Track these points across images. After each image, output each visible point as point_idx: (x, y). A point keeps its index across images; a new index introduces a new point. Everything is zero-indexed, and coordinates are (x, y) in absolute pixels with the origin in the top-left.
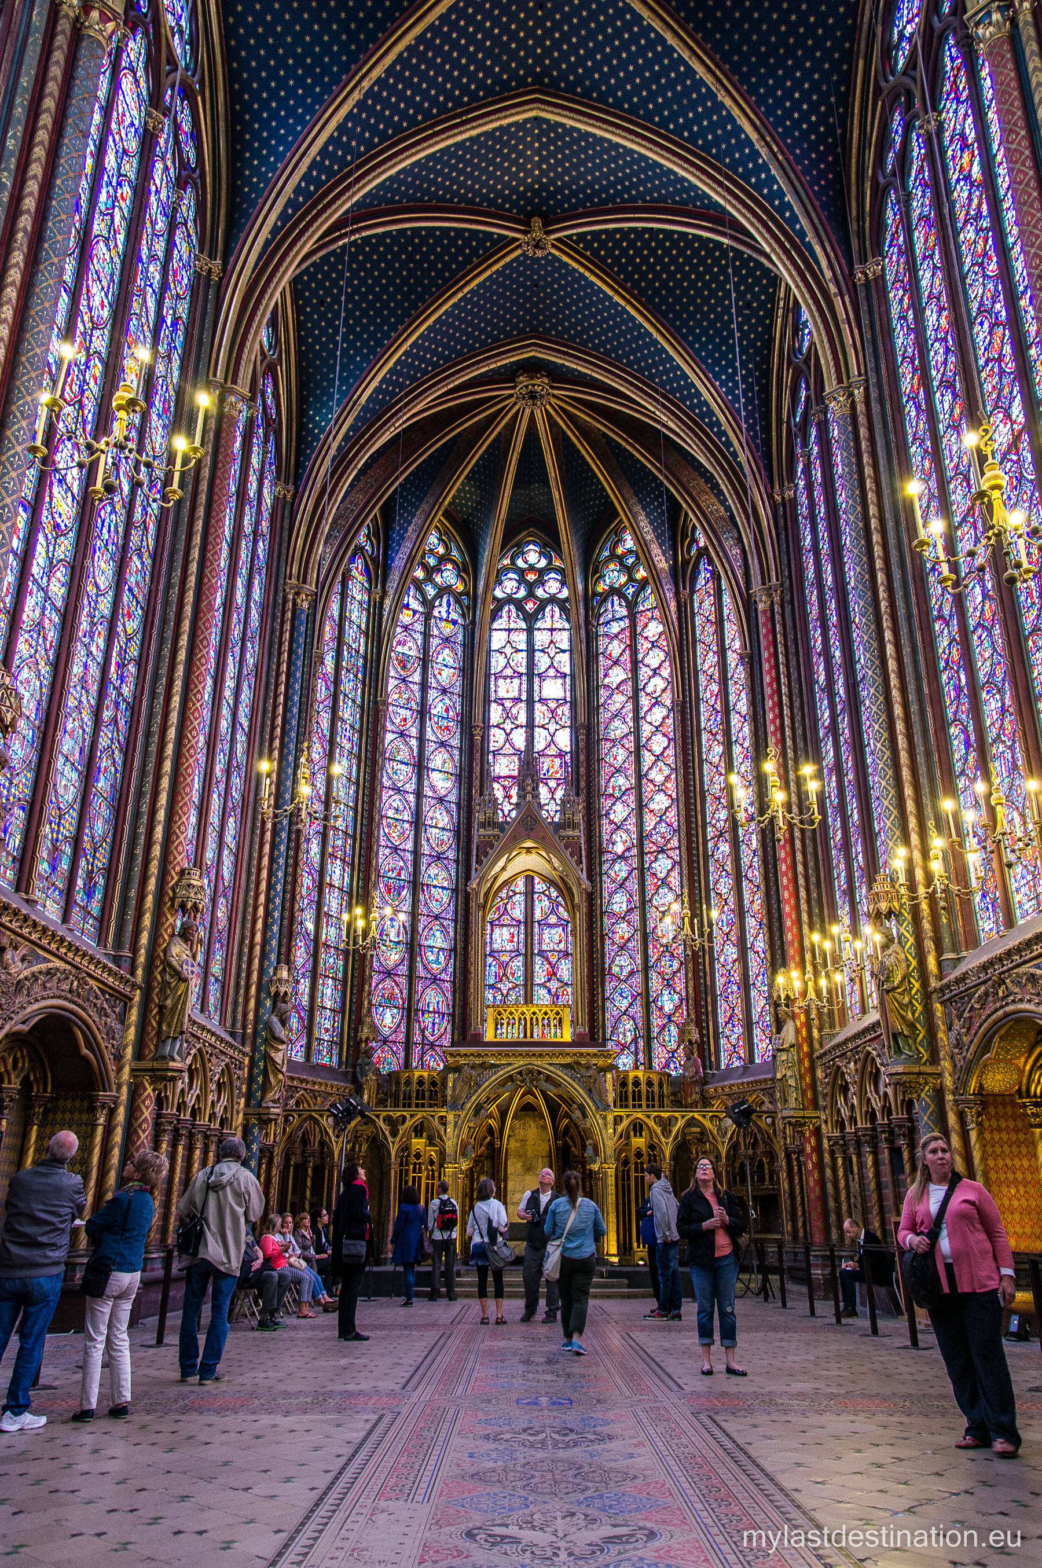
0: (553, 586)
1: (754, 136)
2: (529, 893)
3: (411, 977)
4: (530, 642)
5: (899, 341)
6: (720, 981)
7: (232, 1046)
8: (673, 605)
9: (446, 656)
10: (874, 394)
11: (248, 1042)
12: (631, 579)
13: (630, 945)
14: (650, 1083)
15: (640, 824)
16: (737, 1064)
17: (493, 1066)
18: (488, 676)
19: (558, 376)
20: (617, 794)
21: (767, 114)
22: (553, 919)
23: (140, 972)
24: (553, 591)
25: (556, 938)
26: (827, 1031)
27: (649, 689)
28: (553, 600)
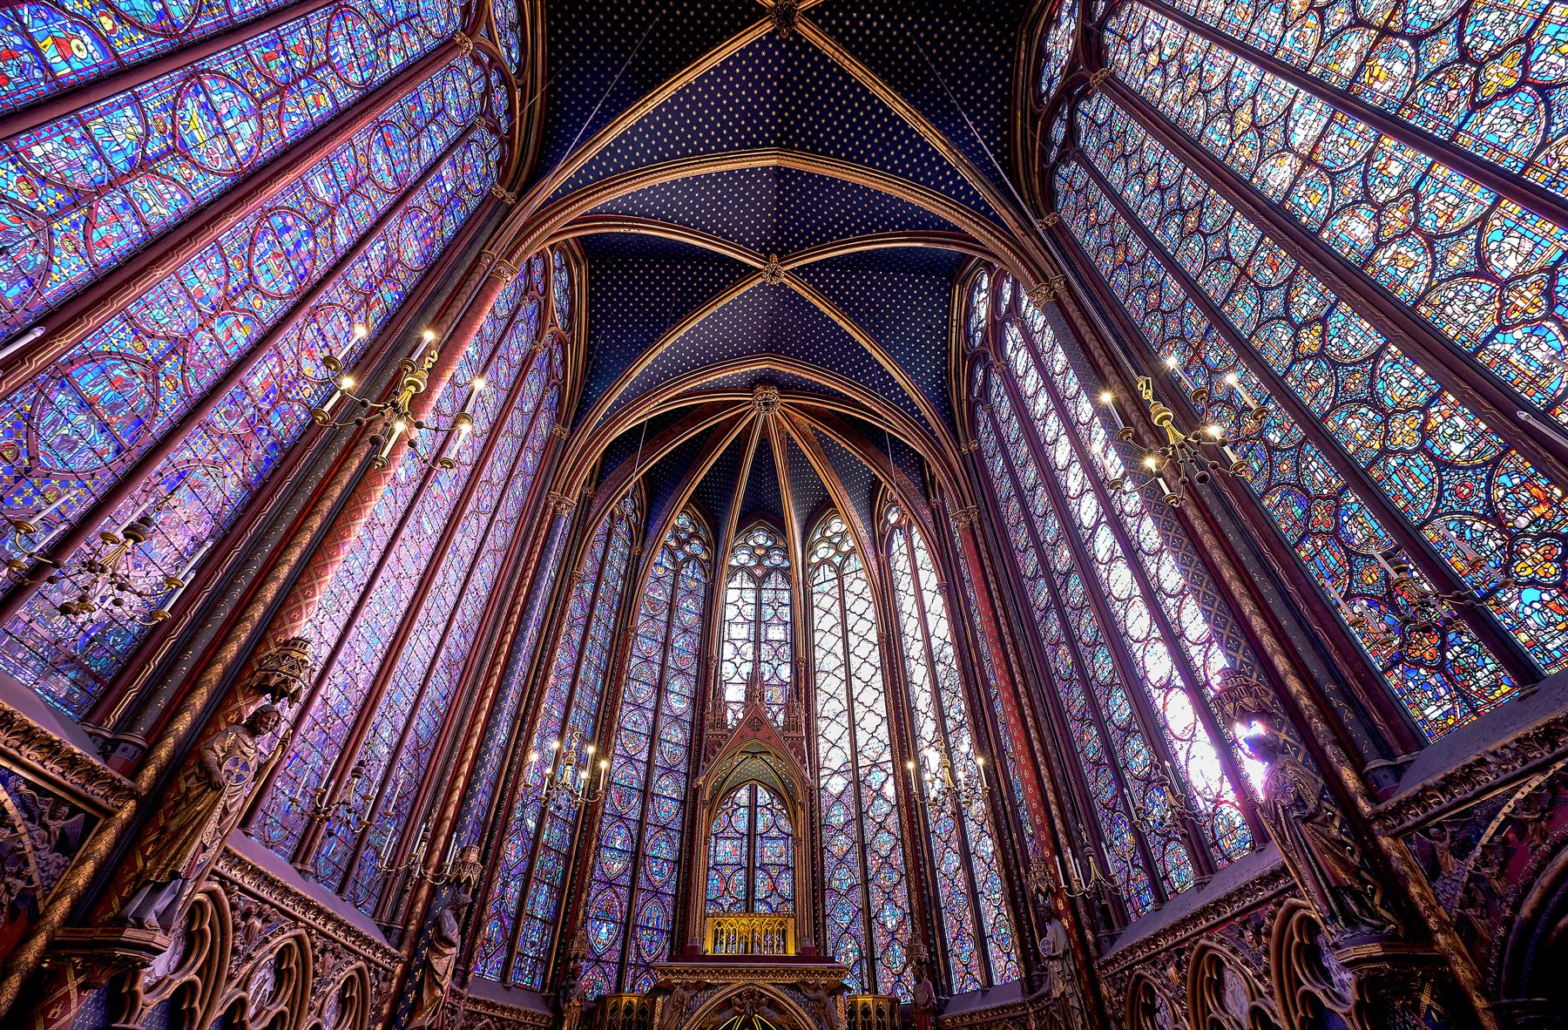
2: (753, 806)
3: (633, 887)
4: (758, 598)
6: (943, 893)
7: (369, 943)
8: (874, 563)
9: (689, 604)
11: (407, 943)
12: (838, 552)
13: (849, 857)
14: (880, 1013)
16: (971, 988)
17: (709, 986)
19: (787, 387)
22: (774, 833)
26: (1103, 933)
28: (776, 568)
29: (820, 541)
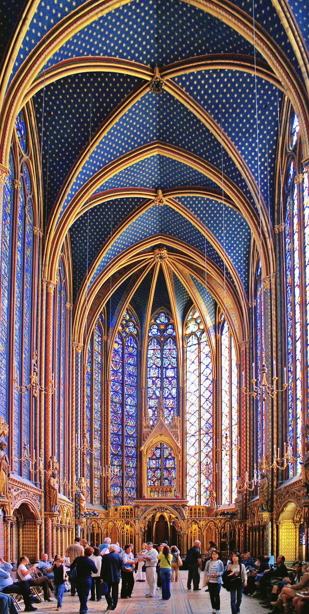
0: (170, 331)
8: (213, 341)
29: (190, 321)
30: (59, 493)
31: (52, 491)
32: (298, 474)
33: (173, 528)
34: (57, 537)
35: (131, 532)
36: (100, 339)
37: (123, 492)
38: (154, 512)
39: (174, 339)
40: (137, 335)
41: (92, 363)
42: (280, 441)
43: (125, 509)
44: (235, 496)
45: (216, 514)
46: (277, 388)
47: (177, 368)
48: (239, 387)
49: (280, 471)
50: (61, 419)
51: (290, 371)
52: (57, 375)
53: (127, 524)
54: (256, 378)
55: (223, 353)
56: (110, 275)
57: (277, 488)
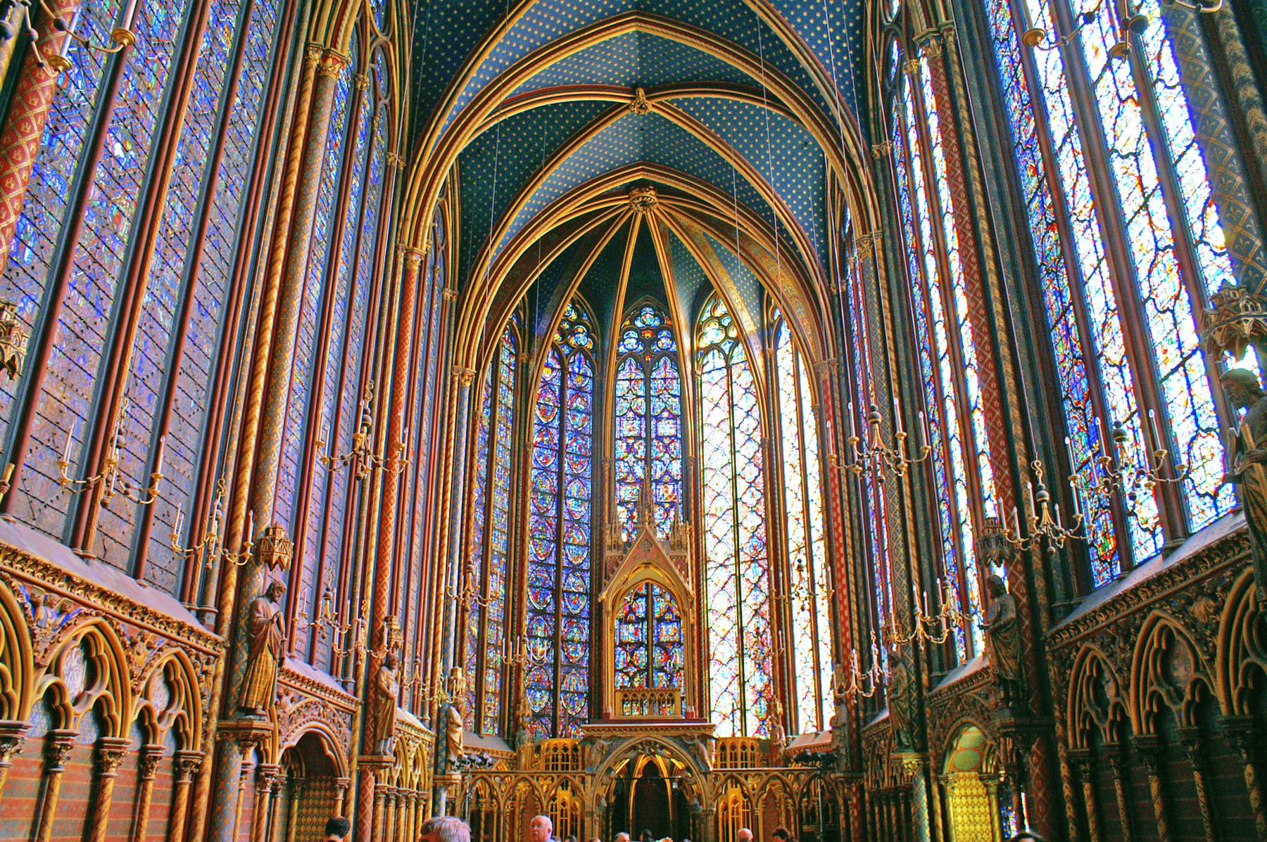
0: (664, 342)
1: (795, 52)
4: (648, 389)
5: (904, 206)
8: (759, 361)
10: (889, 243)
12: (727, 337)
13: (729, 636)
15: (736, 539)
18: (614, 417)
19: (662, 190)
20: (719, 514)
21: (804, 36)
22: (668, 616)
23: (360, 693)
24: (665, 346)
25: (671, 632)
26: (869, 713)
27: (743, 427)
30: (400, 706)
31: (383, 700)
32: (979, 655)
33: (679, 795)
34: (386, 823)
35: (574, 808)
36: (513, 360)
37: (555, 704)
38: (632, 754)
39: (675, 358)
40: (594, 350)
41: (493, 407)
42: (926, 574)
43: (560, 747)
44: (829, 711)
45: (787, 760)
46: (908, 456)
47: (683, 417)
48: (822, 456)
49: (934, 648)
50: (418, 530)
51: (934, 421)
52: (413, 434)
53: (564, 785)
54: (859, 433)
55: (781, 386)
56: (538, 237)
57: (930, 689)
